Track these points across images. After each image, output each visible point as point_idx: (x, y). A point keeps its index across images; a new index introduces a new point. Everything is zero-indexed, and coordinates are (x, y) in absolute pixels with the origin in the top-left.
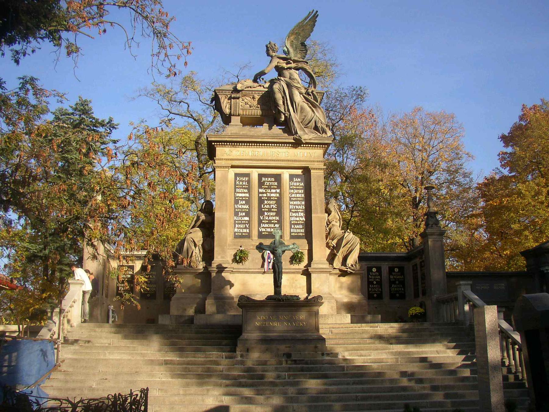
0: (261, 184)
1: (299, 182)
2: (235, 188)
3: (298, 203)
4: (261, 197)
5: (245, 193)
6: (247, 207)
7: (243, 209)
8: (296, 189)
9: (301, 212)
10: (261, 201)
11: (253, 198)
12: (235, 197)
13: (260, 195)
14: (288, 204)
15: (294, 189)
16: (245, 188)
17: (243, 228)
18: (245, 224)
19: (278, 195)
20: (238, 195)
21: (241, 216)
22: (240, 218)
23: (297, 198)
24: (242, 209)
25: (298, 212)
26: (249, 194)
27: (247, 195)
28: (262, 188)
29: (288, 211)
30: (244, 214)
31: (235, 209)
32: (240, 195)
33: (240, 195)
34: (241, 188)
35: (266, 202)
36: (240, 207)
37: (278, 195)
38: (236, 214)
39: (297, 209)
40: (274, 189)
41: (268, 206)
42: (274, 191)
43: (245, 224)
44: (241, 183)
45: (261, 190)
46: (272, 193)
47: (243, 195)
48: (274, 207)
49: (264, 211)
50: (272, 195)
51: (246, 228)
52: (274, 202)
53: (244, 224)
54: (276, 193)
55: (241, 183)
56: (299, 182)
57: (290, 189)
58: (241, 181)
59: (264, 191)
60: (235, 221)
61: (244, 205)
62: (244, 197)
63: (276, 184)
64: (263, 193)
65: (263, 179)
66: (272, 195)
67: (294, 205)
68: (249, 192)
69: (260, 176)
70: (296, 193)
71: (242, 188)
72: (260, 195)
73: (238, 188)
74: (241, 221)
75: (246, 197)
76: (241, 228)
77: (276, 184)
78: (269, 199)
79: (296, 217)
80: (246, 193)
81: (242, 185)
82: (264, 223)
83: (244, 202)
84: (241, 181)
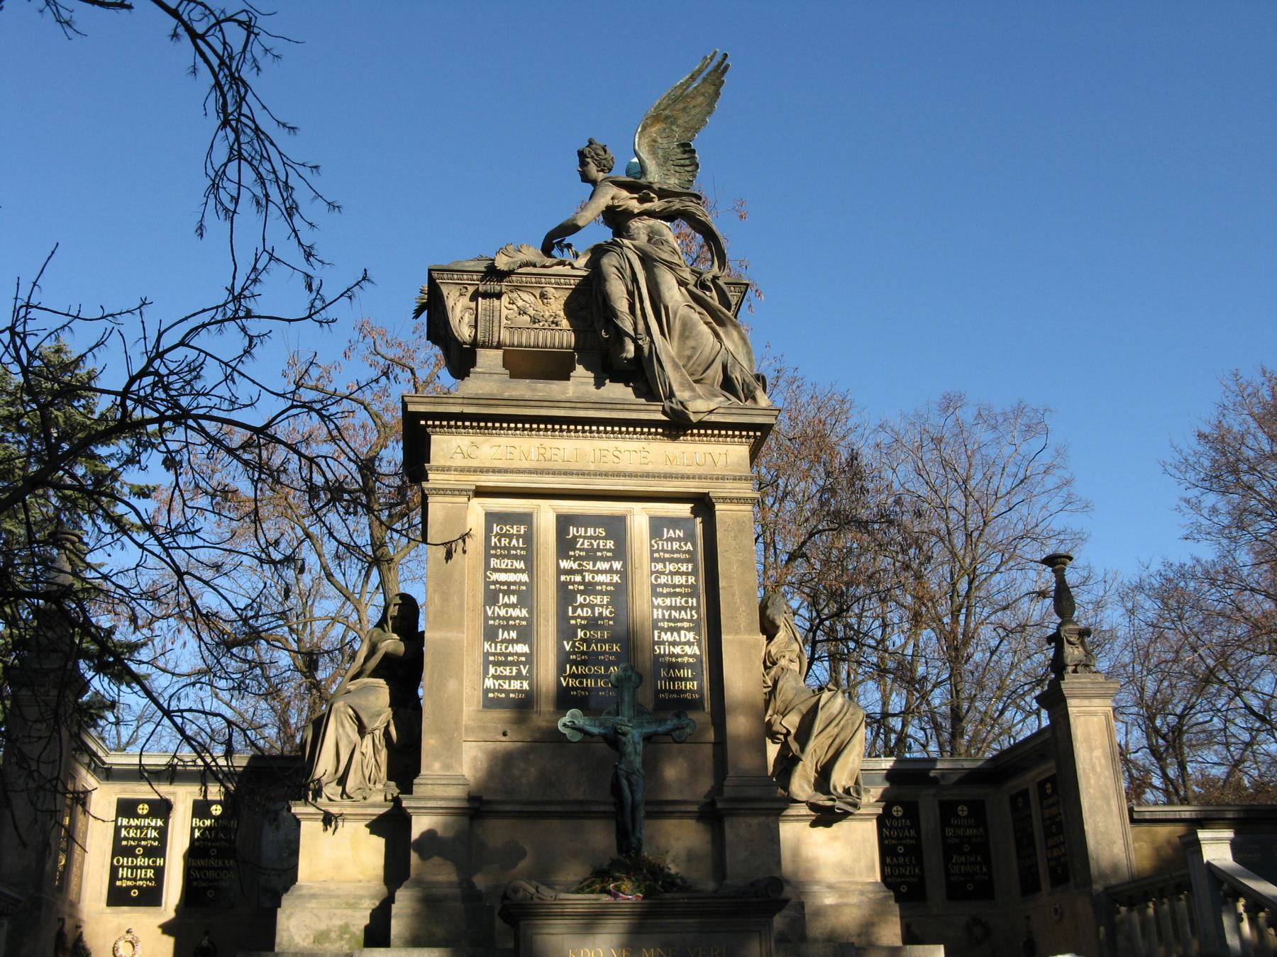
0: (565, 546)
1: (679, 539)
3: (679, 601)
4: (566, 584)
5: (516, 571)
7: (511, 618)
8: (671, 560)
9: (689, 629)
12: (487, 584)
13: (563, 578)
15: (663, 561)
16: (516, 557)
17: (510, 678)
18: (517, 664)
19: (616, 578)
20: (495, 576)
21: (503, 641)
22: (500, 648)
23: (674, 586)
25: (678, 630)
26: (531, 577)
27: (524, 578)
28: (568, 558)
30: (514, 635)
31: (487, 618)
32: (503, 577)
33: (503, 577)
34: (503, 557)
35: (580, 599)
37: (616, 578)
39: (676, 620)
41: (586, 612)
43: (517, 664)
44: (504, 542)
45: (565, 564)
47: (511, 577)
48: (606, 613)
49: (576, 627)
50: (600, 578)
51: (519, 676)
52: (606, 599)
53: (512, 664)
54: (611, 571)
55: (504, 542)
56: (679, 539)
58: (505, 535)
59: (575, 566)
60: (487, 654)
61: (514, 606)
62: (514, 583)
63: (610, 544)
64: (571, 572)
65: (573, 531)
68: (529, 569)
69: (564, 522)
71: (509, 556)
72: (563, 578)
73: (496, 556)
74: (506, 655)
75: (520, 583)
76: (505, 678)
77: (610, 544)
78: (590, 588)
79: (674, 644)
84: (505, 535)
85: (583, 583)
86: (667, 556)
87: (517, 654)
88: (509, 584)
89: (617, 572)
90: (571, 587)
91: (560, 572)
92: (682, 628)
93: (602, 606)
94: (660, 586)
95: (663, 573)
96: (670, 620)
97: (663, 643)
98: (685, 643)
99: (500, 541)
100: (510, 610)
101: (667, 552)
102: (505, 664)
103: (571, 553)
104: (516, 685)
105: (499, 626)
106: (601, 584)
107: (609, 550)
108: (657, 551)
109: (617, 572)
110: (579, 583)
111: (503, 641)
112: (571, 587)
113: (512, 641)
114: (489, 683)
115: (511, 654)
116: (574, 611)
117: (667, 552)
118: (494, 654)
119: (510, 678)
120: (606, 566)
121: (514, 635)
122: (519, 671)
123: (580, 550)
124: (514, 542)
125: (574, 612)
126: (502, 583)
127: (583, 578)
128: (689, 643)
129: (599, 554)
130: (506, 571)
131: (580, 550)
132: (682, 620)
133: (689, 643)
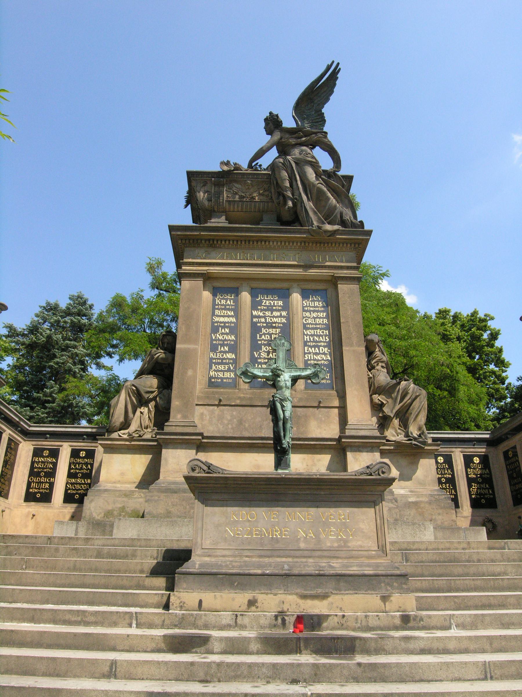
2: (214, 309)
4: (256, 323)
5: (229, 316)
6: (233, 337)
7: (225, 340)
8: (314, 311)
9: (324, 347)
10: (255, 329)
11: (243, 324)
12: (213, 323)
13: (254, 320)
14: (300, 334)
15: (310, 311)
20: (217, 319)
21: (221, 352)
23: (316, 324)
24: (224, 341)
25: (319, 347)
26: (237, 319)
27: (234, 320)
28: (257, 310)
29: (301, 344)
30: (226, 349)
31: (212, 340)
32: (222, 319)
33: (222, 319)
34: (222, 309)
35: (264, 331)
36: (221, 338)
37: (284, 320)
38: (214, 348)
39: (317, 342)
40: (276, 310)
41: (267, 337)
42: (276, 314)
45: (255, 313)
46: (274, 317)
47: (226, 319)
49: (261, 344)
50: (275, 320)
51: (229, 370)
52: (278, 330)
54: (281, 316)
57: (304, 311)
59: (261, 314)
60: (211, 359)
61: (227, 334)
62: (228, 322)
64: (259, 317)
66: (275, 320)
67: (312, 335)
68: (237, 315)
70: (314, 318)
71: (225, 309)
72: (254, 320)
73: (218, 309)
74: (222, 359)
75: (231, 322)
76: (221, 371)
78: (270, 326)
79: (316, 354)
80: (232, 316)
81: (225, 306)
82: (261, 363)
83: (227, 331)
85: (266, 322)
86: (311, 309)
87: (228, 358)
88: (225, 323)
89: (284, 317)
90: (259, 325)
91: (253, 317)
92: (321, 346)
93: (276, 334)
94: (308, 324)
95: (309, 318)
96: (314, 341)
97: (310, 353)
98: (322, 354)
99: (221, 302)
100: (225, 336)
101: (312, 307)
102: (222, 363)
103: (259, 308)
104: (227, 375)
105: (219, 344)
106: (275, 323)
107: (280, 306)
108: (306, 306)
109: (284, 317)
110: (263, 323)
111: (221, 352)
112: (259, 325)
113: (225, 352)
114: (212, 374)
115: (224, 359)
116: (260, 336)
117: (312, 307)
118: (215, 359)
119: (223, 371)
120: (278, 314)
121: (226, 349)
122: (229, 367)
123: (264, 306)
124: (228, 302)
125: (260, 336)
126: (221, 322)
127: (266, 320)
128: (324, 354)
129: (274, 308)
130: (224, 316)
131: (264, 306)
132: (321, 342)
133: (324, 354)
